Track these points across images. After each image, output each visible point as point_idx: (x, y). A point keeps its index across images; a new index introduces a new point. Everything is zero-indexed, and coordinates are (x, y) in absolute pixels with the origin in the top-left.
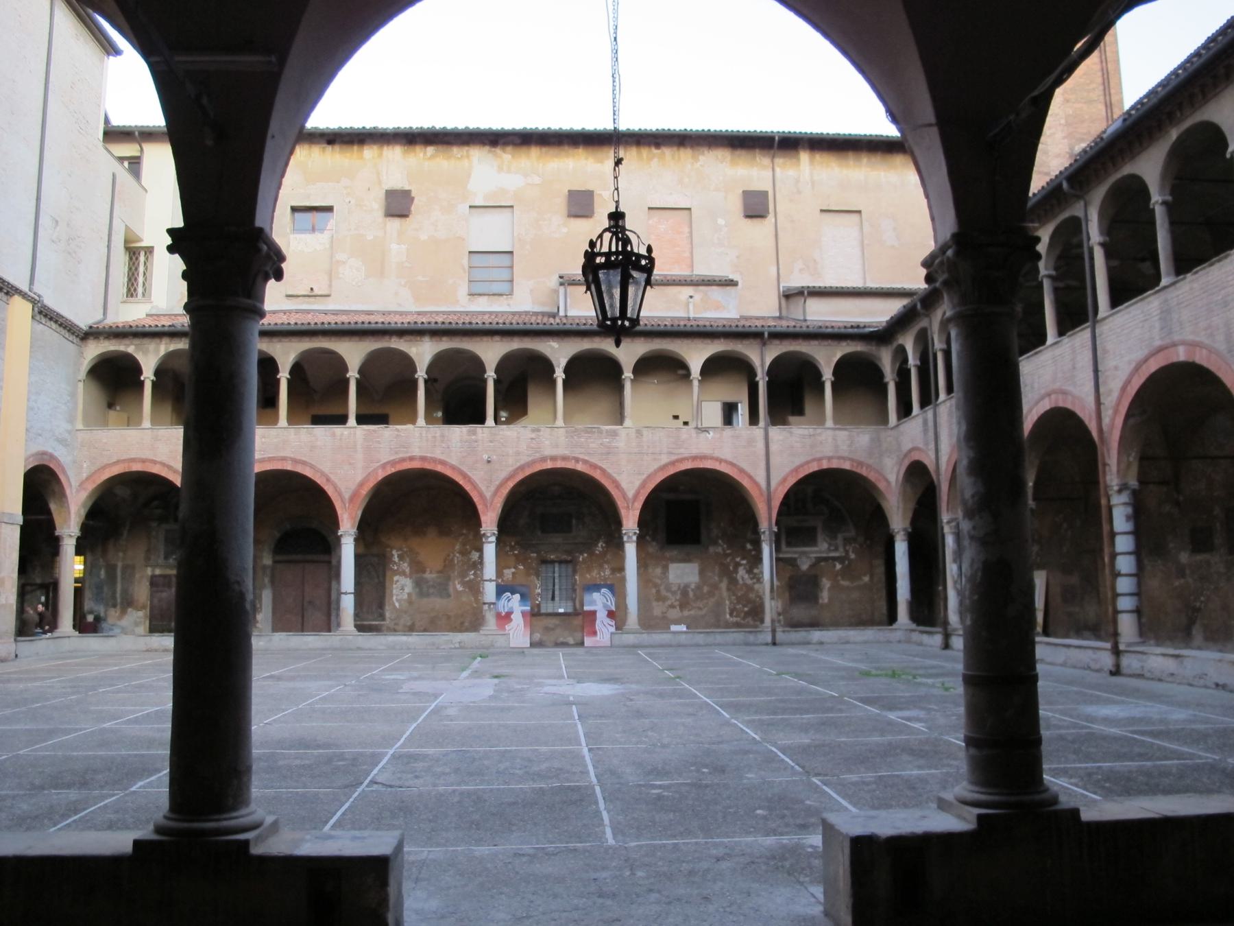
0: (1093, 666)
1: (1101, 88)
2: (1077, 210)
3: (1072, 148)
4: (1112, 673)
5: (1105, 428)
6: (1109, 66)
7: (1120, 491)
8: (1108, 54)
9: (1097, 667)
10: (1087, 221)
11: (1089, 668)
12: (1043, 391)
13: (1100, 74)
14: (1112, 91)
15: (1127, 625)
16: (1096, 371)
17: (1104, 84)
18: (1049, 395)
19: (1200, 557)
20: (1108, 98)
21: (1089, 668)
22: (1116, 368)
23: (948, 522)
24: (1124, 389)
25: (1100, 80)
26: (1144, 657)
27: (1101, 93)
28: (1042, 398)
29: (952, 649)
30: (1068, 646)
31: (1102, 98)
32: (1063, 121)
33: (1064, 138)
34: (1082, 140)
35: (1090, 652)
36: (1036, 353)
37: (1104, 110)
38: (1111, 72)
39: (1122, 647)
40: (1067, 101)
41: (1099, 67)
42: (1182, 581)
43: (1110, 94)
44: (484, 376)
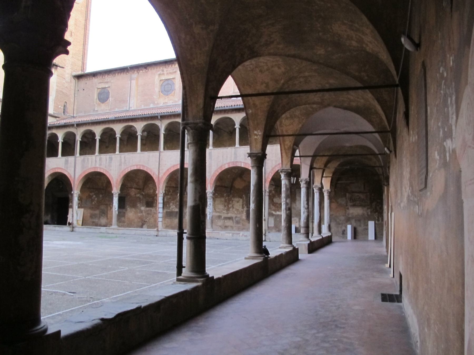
0: (146, 234)
1: (82, 57)
2: (157, 123)
3: (72, 73)
4: (157, 236)
5: (160, 178)
6: (85, 51)
7: (161, 193)
8: (86, 47)
9: (149, 234)
10: (161, 127)
11: (145, 235)
12: (134, 164)
13: (82, 52)
14: (85, 59)
15: (160, 224)
16: (159, 164)
17: (83, 56)
18: (137, 166)
19: (148, 209)
20: (83, 61)
21: (145, 235)
22: (166, 164)
23: (76, 194)
24: (168, 170)
25: (82, 54)
26: (167, 232)
27: (81, 58)
28: (134, 165)
29: (75, 231)
30: (137, 230)
31: (81, 60)
32: (71, 63)
33: (70, 69)
34: (75, 71)
35: (146, 231)
36: (132, 153)
37: (81, 64)
38: (85, 53)
39: (159, 230)
40: (73, 57)
41: (82, 50)
42: (141, 214)
43: (84, 60)
44: (58, 141)
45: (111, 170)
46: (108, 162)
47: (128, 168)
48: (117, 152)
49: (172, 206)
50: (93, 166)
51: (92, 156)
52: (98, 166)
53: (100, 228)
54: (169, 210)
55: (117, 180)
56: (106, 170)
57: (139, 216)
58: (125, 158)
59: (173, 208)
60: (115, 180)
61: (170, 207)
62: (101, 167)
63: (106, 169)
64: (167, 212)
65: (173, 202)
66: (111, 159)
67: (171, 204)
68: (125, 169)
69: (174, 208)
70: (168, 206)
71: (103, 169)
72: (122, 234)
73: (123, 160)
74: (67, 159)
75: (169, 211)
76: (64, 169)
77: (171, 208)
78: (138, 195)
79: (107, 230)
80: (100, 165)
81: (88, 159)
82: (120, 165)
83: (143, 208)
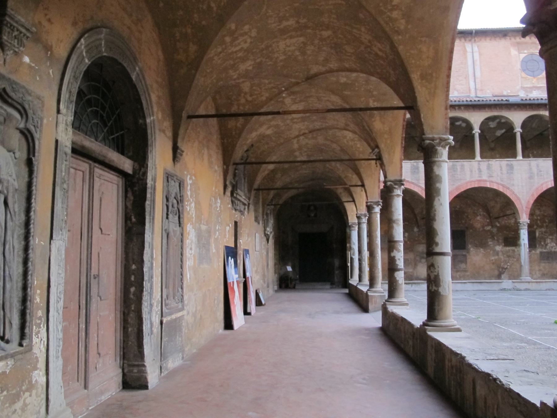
19: (508, 248)
42: (497, 257)
45: (513, 185)
46: (505, 171)
47: (547, 182)
48: (520, 157)
49: (551, 243)
50: (476, 177)
51: (470, 161)
52: (485, 177)
53: (502, 282)
54: (545, 249)
55: (528, 202)
56: (503, 186)
57: (492, 260)
58: (538, 166)
59: (552, 247)
60: (524, 203)
61: (547, 245)
62: (493, 179)
63: (502, 183)
64: (541, 253)
65: (551, 237)
66: (511, 167)
67: (548, 241)
68: (542, 185)
69: (554, 246)
70: (542, 243)
71: (498, 184)
72: (546, 290)
73: (535, 170)
74: (415, 164)
75: (545, 251)
76: (413, 183)
77: (548, 247)
78: (489, 228)
79: (516, 284)
80: (491, 176)
81: (462, 166)
82: (531, 177)
83: (498, 248)
